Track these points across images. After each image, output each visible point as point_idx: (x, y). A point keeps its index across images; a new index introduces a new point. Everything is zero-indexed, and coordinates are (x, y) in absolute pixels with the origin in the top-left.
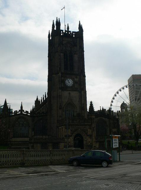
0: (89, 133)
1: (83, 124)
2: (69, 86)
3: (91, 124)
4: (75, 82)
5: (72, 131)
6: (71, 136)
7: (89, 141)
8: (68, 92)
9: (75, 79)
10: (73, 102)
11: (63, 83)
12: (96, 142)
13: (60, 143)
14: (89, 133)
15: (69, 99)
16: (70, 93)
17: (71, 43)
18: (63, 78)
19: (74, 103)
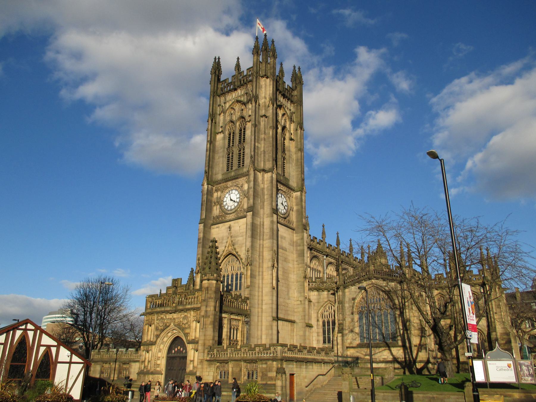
1: (181, 307)
2: (231, 210)
3: (199, 305)
5: (157, 329)
6: (153, 343)
7: (192, 359)
8: (227, 224)
9: (246, 187)
10: (235, 249)
11: (218, 206)
12: (207, 360)
13: (133, 364)
14: (192, 336)
15: (227, 242)
16: (230, 227)
17: (242, 99)
18: (219, 193)
19: (237, 253)
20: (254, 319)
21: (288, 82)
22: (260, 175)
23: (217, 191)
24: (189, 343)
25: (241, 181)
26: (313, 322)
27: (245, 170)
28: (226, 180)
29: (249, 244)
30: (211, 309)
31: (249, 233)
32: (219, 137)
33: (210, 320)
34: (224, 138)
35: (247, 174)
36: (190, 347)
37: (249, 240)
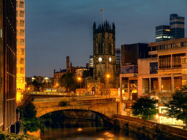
0: (97, 87)
4: (103, 59)
14: (97, 87)
20: (106, 83)
21: (112, 28)
22: (106, 56)
23: (97, 57)
24: (96, 88)
25: (102, 56)
26: (117, 83)
27: (103, 54)
28: (99, 55)
29: (104, 70)
30: (99, 83)
31: (104, 68)
32: (97, 44)
33: (99, 85)
34: (98, 45)
35: (103, 55)
36: (96, 89)
37: (104, 69)
